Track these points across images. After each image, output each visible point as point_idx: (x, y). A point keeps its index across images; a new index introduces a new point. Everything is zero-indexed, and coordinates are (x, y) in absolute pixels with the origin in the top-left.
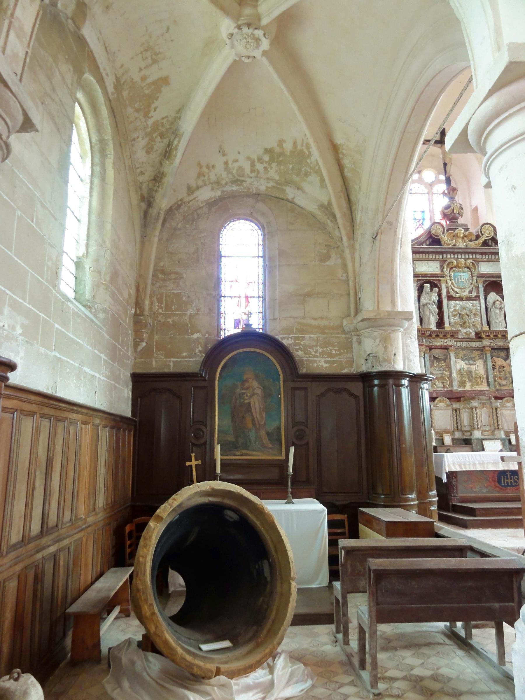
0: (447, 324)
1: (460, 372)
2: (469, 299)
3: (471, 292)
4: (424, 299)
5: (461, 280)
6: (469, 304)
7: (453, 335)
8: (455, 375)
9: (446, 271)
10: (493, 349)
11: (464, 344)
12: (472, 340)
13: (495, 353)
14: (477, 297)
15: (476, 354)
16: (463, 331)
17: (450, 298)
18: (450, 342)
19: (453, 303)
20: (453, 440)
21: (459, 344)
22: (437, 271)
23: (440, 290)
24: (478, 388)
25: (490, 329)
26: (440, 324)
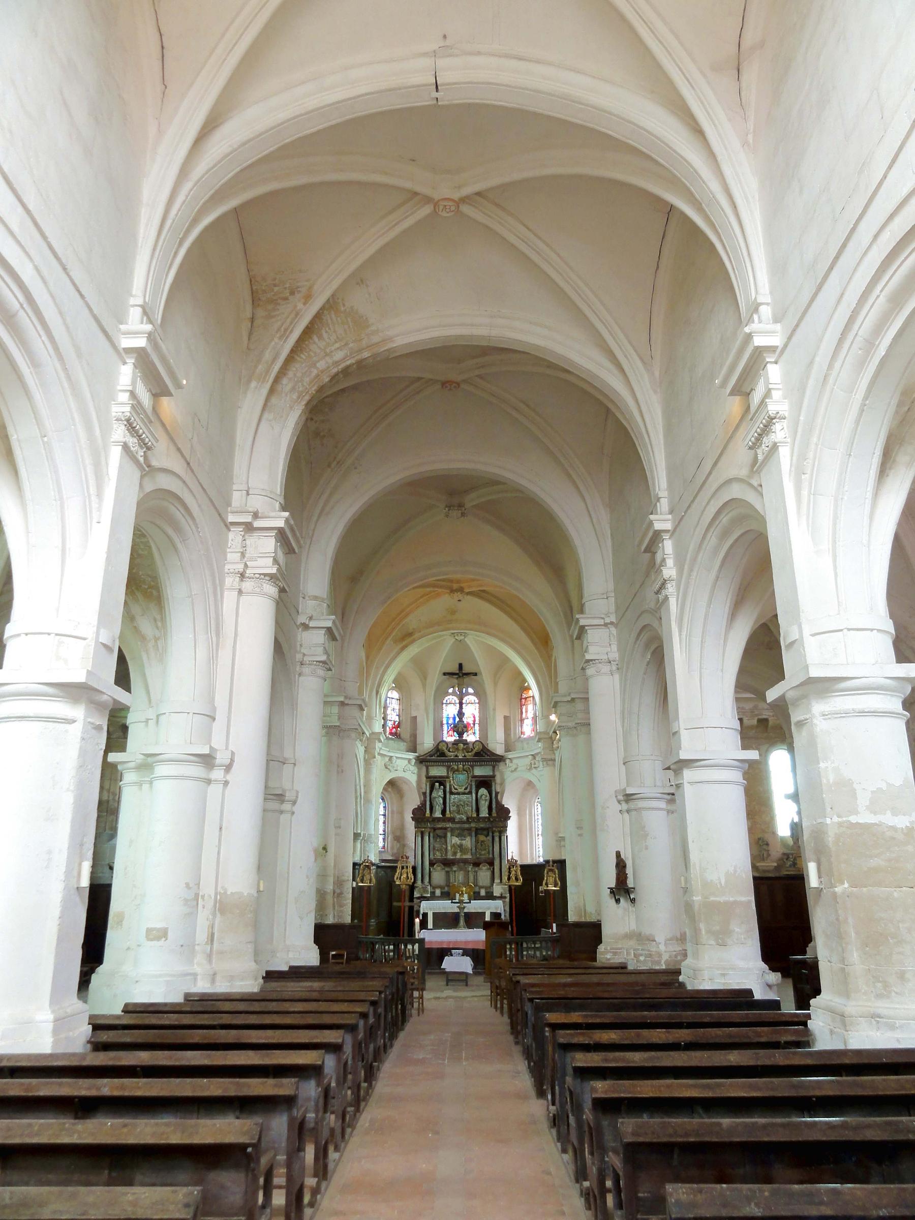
0: (448, 812)
1: (453, 846)
2: (464, 794)
3: (466, 789)
4: (434, 795)
5: (459, 780)
6: (464, 797)
7: (452, 820)
8: (449, 848)
9: (451, 774)
10: (477, 829)
11: (458, 826)
12: (464, 823)
13: (479, 832)
14: (470, 793)
15: (466, 832)
16: (458, 816)
17: (451, 793)
18: (449, 825)
19: (453, 797)
20: (442, 893)
21: (454, 826)
22: (445, 774)
23: (445, 787)
24: (464, 857)
25: (478, 815)
26: (444, 812)
